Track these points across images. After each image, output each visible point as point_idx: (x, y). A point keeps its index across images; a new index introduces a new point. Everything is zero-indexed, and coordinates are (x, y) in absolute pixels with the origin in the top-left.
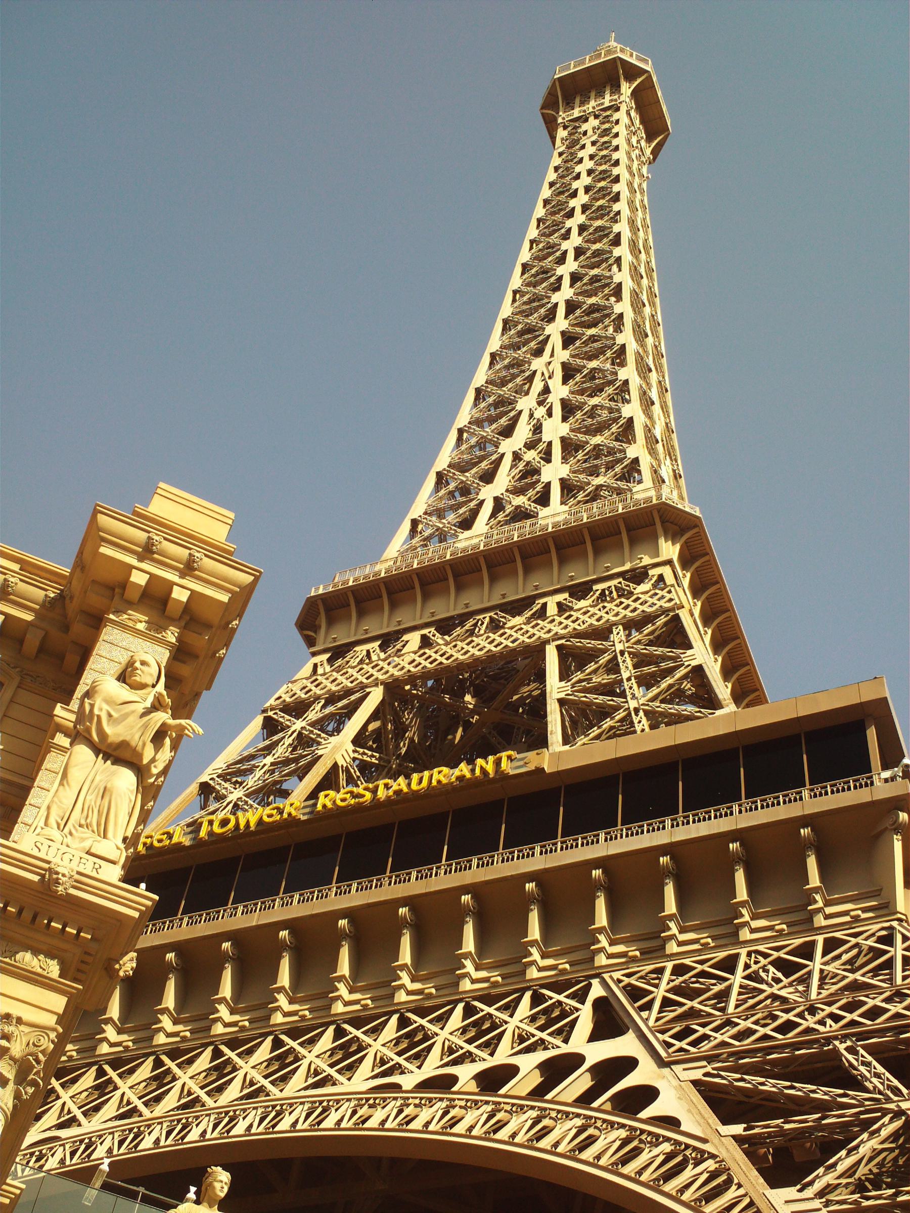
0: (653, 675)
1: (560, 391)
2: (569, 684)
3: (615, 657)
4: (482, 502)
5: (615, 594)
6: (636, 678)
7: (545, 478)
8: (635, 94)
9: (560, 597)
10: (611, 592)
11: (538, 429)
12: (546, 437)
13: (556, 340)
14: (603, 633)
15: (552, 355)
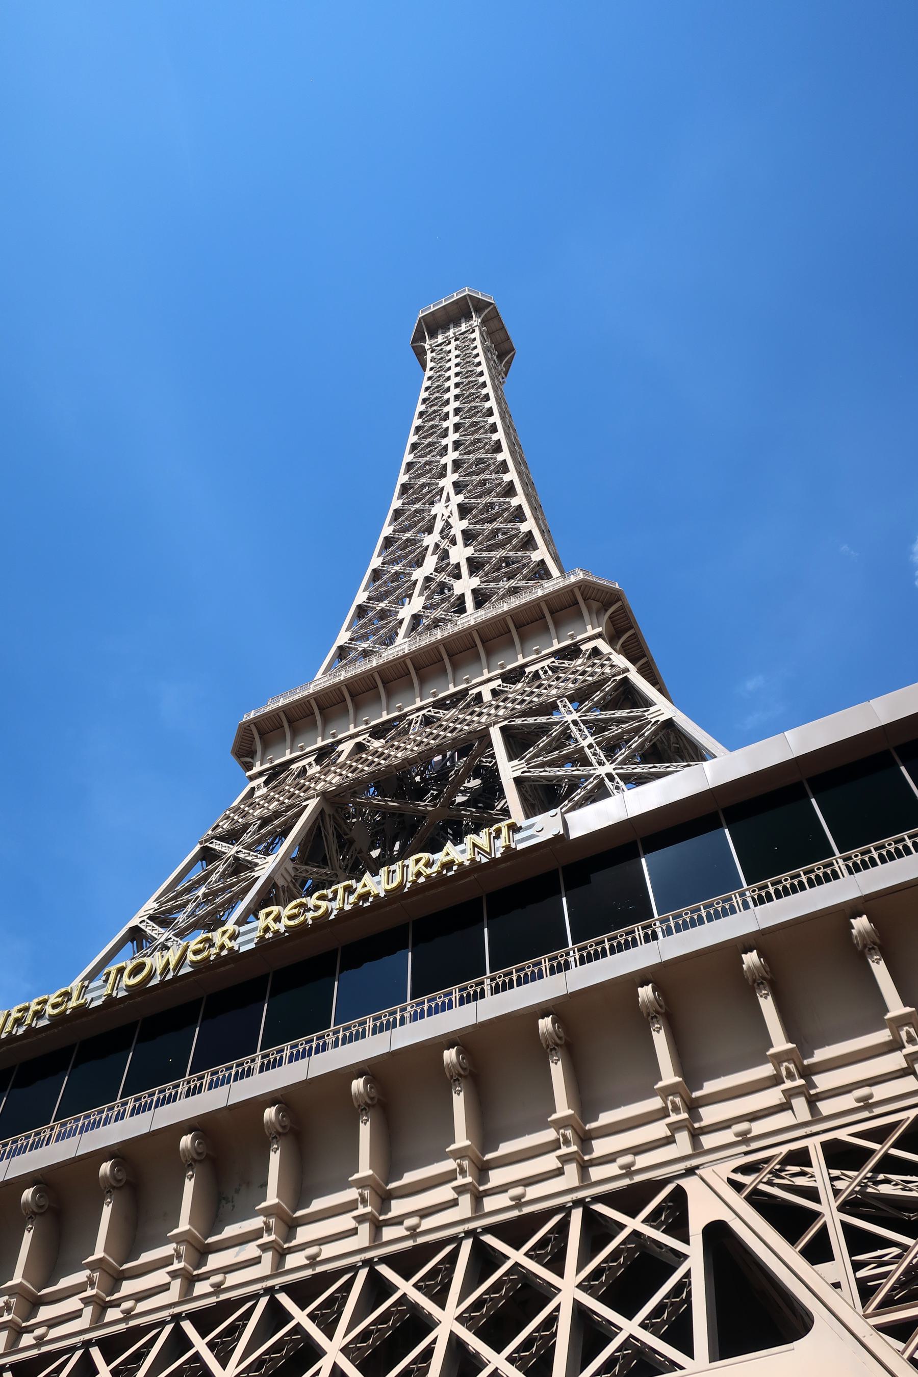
0: (619, 737)
1: (459, 526)
2: (523, 761)
3: (568, 728)
4: (401, 622)
5: (550, 672)
6: (598, 744)
7: (457, 591)
8: (484, 322)
9: (494, 684)
10: (546, 672)
11: (445, 555)
12: (453, 560)
13: (449, 489)
14: (550, 708)
15: (448, 500)
